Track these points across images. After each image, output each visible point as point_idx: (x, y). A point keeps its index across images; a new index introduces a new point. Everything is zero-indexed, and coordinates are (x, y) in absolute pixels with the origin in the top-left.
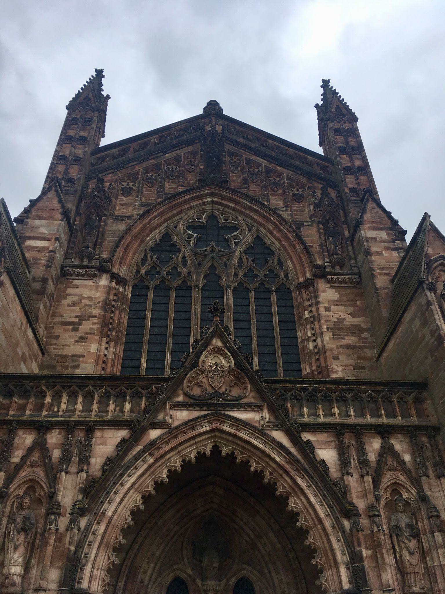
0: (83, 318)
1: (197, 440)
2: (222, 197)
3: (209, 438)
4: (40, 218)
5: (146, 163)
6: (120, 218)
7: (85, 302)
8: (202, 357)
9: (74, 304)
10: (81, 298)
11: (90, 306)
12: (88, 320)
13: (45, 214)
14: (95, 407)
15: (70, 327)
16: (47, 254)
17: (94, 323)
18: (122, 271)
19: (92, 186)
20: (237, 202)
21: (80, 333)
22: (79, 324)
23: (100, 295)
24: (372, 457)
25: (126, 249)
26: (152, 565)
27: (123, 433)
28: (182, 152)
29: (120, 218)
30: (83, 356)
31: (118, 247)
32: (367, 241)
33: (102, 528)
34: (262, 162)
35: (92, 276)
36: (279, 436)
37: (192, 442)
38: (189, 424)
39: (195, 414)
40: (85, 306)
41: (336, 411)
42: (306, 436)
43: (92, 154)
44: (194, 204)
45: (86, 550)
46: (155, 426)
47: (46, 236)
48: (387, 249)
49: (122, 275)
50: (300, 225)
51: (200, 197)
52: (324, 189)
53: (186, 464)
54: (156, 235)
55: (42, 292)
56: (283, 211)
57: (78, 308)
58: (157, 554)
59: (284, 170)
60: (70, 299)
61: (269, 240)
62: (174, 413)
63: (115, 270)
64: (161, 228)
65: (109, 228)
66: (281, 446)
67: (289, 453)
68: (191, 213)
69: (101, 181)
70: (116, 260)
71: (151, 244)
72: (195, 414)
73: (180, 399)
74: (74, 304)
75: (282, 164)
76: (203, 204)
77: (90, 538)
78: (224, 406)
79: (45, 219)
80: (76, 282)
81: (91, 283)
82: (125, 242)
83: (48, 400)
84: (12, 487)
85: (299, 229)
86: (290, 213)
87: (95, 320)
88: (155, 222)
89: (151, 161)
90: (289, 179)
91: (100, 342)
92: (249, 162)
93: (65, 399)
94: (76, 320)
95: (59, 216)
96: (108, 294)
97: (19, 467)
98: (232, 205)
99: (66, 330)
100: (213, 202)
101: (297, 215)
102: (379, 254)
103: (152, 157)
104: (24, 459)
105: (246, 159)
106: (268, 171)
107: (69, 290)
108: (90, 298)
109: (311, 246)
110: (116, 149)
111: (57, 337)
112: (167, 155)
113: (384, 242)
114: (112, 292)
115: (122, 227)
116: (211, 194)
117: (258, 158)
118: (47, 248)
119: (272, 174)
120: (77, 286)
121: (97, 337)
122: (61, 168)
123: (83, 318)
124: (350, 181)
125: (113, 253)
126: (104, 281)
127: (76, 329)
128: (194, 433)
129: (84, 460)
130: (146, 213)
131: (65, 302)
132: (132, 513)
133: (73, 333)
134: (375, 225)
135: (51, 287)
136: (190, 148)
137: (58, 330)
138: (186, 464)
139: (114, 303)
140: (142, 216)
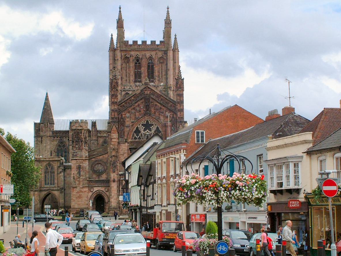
0: (124, 153)
4: (113, 133)
6: (127, 127)
7: (124, 149)
9: (122, 150)
10: (123, 149)
13: (114, 132)
19: (120, 117)
22: (124, 154)
28: (139, 103)
29: (127, 127)
31: (128, 135)
35: (124, 144)
44: (143, 119)
47: (116, 138)
51: (145, 118)
52: (173, 115)
57: (123, 151)
61: (160, 129)
65: (125, 130)
69: (122, 115)
74: (122, 150)
75: (164, 106)
79: (115, 133)
80: (122, 145)
81: (124, 145)
87: (126, 154)
89: (132, 107)
92: (156, 105)
94: (123, 154)
95: (117, 133)
98: (152, 119)
99: (122, 156)
106: (161, 108)
107: (120, 147)
108: (125, 149)
111: (120, 158)
112: (136, 104)
115: (128, 129)
116: (147, 117)
117: (158, 104)
118: (116, 141)
120: (122, 146)
122: (113, 114)
123: (124, 153)
124: (179, 114)
125: (127, 137)
126: (127, 144)
127: (123, 156)
133: (123, 157)
136: (142, 101)
137: (120, 156)
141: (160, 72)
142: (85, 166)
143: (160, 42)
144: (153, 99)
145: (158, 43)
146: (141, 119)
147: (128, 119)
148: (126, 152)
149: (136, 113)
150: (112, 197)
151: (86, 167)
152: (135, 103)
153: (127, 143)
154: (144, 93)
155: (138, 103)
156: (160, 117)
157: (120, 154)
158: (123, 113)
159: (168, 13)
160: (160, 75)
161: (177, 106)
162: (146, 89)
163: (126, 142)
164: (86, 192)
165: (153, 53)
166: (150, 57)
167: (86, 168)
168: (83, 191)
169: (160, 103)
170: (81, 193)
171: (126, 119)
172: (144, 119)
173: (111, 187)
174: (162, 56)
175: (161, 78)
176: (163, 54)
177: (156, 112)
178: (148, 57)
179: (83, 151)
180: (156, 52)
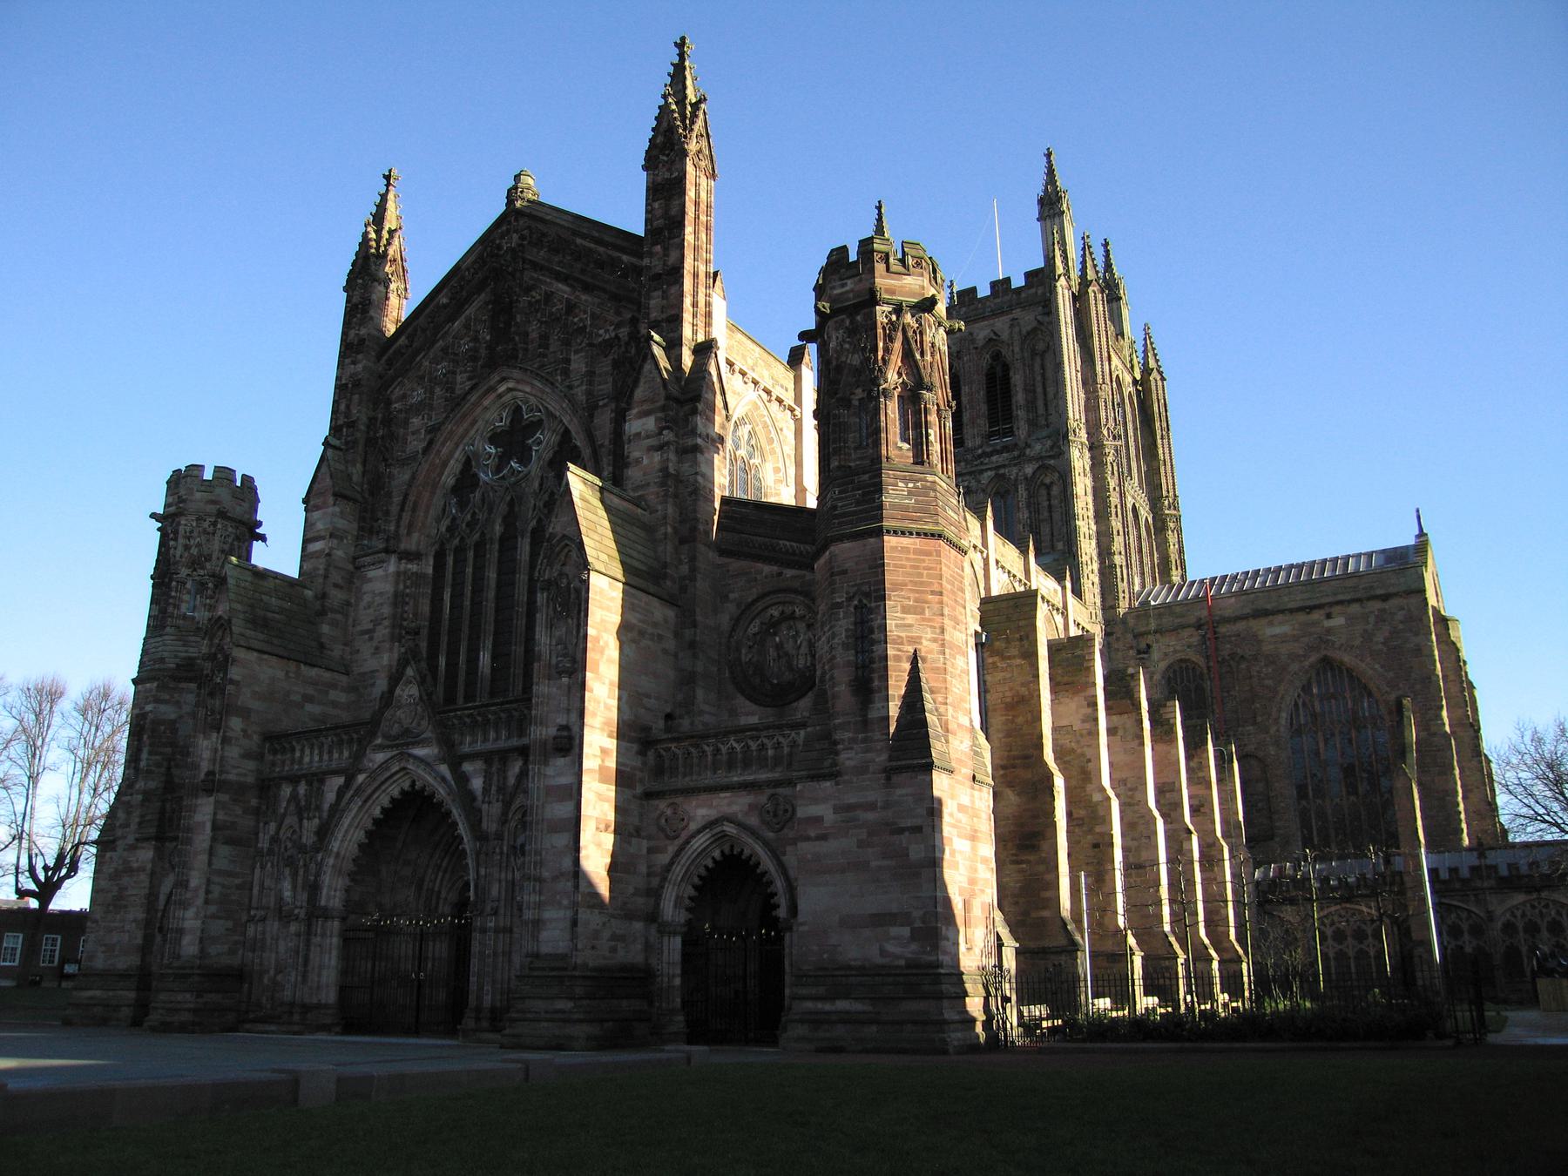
1: (395, 778)
2: (518, 382)
3: (404, 775)
5: (432, 350)
6: (403, 463)
7: (378, 600)
8: (398, 691)
11: (382, 604)
12: (380, 624)
14: (326, 757)
15: (367, 636)
16: (324, 560)
17: (385, 628)
18: (411, 543)
20: (533, 386)
21: (375, 643)
23: (388, 588)
24: (512, 781)
25: (414, 510)
26: (440, 874)
27: (341, 780)
28: (470, 311)
30: (377, 671)
32: (630, 441)
33: (331, 861)
34: (565, 293)
36: (444, 769)
37: (391, 781)
38: (384, 765)
39: (389, 754)
40: (378, 605)
41: (492, 735)
42: (467, 767)
43: (379, 358)
44: (486, 403)
45: (323, 877)
46: (360, 771)
47: (323, 534)
48: (652, 449)
49: (413, 548)
50: (592, 408)
51: (492, 389)
53: (393, 800)
54: (454, 466)
55: (322, 613)
56: (578, 386)
57: (371, 611)
58: (444, 864)
59: (590, 299)
60: (367, 598)
62: (372, 756)
63: (403, 546)
64: (456, 455)
66: (443, 779)
67: (449, 786)
68: (488, 415)
69: (389, 403)
70: (403, 531)
71: (451, 481)
72: (389, 754)
73: (379, 741)
75: (587, 288)
76: (500, 396)
77: (325, 868)
78: (407, 744)
80: (371, 574)
82: (412, 498)
83: (298, 754)
84: (282, 832)
85: (591, 416)
86: (584, 387)
88: (445, 451)
89: (438, 345)
90: (593, 316)
91: (391, 650)
93: (307, 752)
94: (370, 626)
96: (397, 583)
97: (284, 815)
100: (509, 390)
101: (600, 384)
102: (638, 461)
103: (439, 335)
104: (286, 808)
105: (546, 292)
107: (367, 587)
108: (381, 594)
109: (602, 446)
110: (403, 338)
113: (648, 437)
114: (402, 578)
115: (407, 477)
116: (504, 379)
117: (560, 285)
119: (577, 311)
120: (370, 580)
121: (387, 645)
122: (342, 407)
123: (377, 622)
127: (371, 639)
128: (388, 774)
129: (318, 808)
130: (431, 443)
131: (363, 604)
132: (359, 846)
134: (645, 407)
135: (337, 596)
138: (393, 800)
139: (408, 591)
140: (426, 451)
141: (1039, 390)
142: (173, 716)
143: (1028, 275)
144: (535, 266)
145: (1018, 282)
146: (473, 398)
147: (416, 421)
148: (386, 610)
149: (454, 373)
150: (189, 895)
151: (174, 722)
152: (452, 319)
153: (393, 559)
154: (499, 247)
155: (467, 312)
156: (568, 361)
157: (359, 628)
158: (398, 392)
159: (1050, 172)
160: (1040, 403)
161: (651, 254)
162: (509, 223)
163: (387, 551)
164: (144, 870)
165: (1001, 324)
166: (990, 340)
167: (174, 731)
168: (135, 865)
169: (565, 279)
170: (126, 880)
171: (406, 422)
172: (493, 396)
173: (189, 830)
174: (1035, 324)
175: (1041, 410)
176: (1039, 318)
177: (551, 341)
178: (980, 343)
179: (168, 629)
180: (1011, 316)
